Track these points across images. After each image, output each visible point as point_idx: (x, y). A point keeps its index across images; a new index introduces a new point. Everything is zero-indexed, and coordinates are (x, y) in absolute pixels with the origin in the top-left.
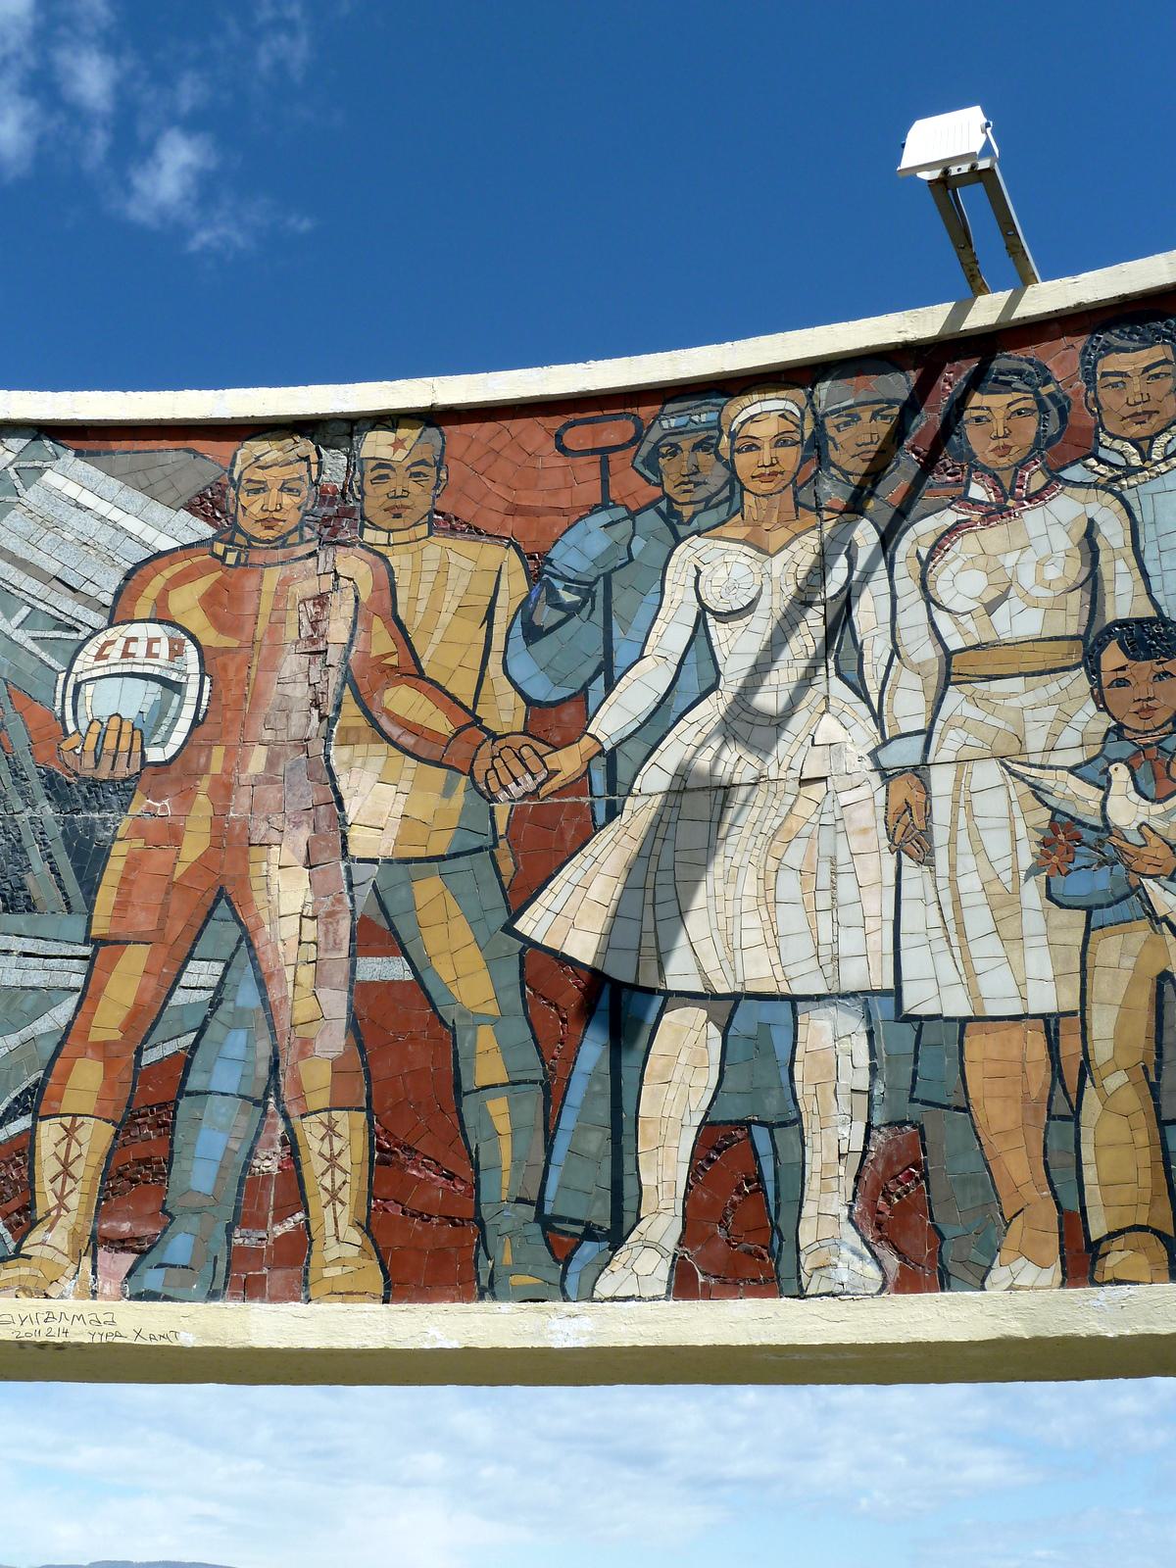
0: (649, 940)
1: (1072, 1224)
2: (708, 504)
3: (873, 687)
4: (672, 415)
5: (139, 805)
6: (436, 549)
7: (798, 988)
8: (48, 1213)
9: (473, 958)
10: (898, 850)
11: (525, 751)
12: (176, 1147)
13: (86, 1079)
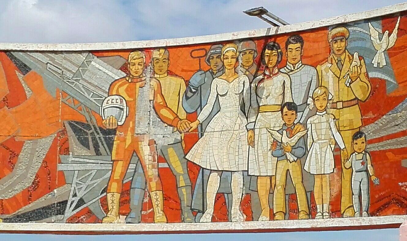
0: (208, 160)
1: (271, 210)
2: (219, 71)
3: (246, 112)
4: (213, 49)
6: (169, 78)
8: (111, 210)
10: (249, 145)
11: (187, 123)
12: (131, 198)
13: (114, 187)
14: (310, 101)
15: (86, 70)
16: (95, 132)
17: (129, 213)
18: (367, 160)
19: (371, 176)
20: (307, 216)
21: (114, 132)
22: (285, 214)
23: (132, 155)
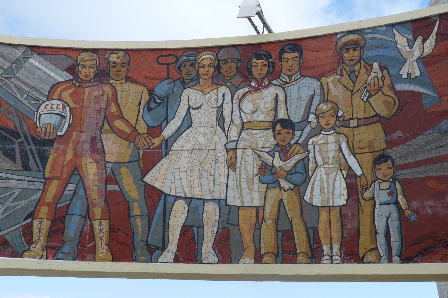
0: (173, 184)
2: (192, 80)
3: (226, 129)
5: (56, 145)
6: (128, 86)
7: (205, 197)
8: (36, 241)
9: (134, 186)
10: (229, 167)
11: (147, 138)
12: (66, 226)
13: (44, 211)
14: (312, 117)
15: (21, 68)
16: (25, 141)
17: (60, 248)
18: (396, 190)
19: (403, 211)
20: (308, 259)
21: (51, 143)
22: (277, 256)
23: (73, 174)
